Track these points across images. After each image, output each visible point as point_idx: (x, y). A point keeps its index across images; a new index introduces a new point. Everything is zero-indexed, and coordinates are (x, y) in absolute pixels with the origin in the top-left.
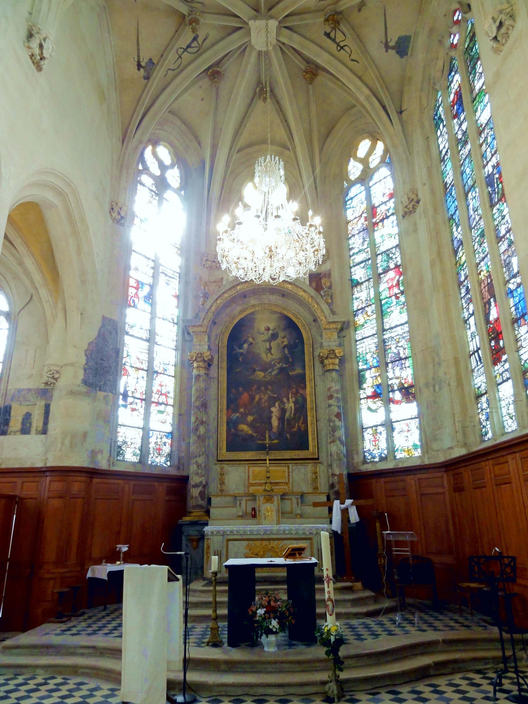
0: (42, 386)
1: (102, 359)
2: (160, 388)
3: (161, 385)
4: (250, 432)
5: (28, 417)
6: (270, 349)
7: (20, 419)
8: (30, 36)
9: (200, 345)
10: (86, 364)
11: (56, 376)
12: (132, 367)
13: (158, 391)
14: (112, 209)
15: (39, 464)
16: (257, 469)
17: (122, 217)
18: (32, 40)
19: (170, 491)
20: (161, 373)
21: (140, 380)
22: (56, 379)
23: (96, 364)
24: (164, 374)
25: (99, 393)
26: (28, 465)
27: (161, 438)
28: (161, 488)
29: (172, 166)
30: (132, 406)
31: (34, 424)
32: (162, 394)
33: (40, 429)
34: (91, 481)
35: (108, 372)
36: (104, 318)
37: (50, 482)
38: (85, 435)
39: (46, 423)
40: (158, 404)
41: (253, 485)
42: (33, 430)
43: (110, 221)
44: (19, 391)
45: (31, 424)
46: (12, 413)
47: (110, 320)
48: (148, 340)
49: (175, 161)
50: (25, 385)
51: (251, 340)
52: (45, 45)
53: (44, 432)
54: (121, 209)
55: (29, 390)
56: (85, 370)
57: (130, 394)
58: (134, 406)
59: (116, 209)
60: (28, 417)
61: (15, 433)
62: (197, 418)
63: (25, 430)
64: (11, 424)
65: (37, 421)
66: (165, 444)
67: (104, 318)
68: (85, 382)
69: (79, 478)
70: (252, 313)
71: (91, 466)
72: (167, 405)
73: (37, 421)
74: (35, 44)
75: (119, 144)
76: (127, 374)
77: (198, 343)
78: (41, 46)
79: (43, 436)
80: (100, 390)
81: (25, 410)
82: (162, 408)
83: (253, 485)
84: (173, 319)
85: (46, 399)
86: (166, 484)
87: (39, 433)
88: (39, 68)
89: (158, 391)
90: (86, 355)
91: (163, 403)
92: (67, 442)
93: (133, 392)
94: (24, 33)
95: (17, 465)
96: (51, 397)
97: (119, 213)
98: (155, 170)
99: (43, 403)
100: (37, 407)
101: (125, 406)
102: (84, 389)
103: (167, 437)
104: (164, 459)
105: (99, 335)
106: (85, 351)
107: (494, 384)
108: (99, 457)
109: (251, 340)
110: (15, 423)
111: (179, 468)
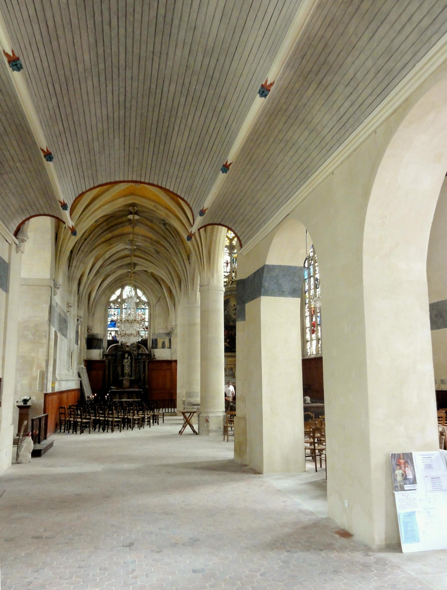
4: (228, 345)
5: (163, 343)
6: (235, 313)
7: (161, 343)
15: (169, 359)
16: (230, 359)
26: (166, 359)
33: (169, 346)
41: (229, 365)
44: (160, 333)
51: (228, 309)
55: (163, 333)
60: (163, 343)
61: (160, 348)
63: (163, 347)
65: (167, 344)
70: (228, 299)
73: (167, 344)
79: (170, 349)
83: (229, 365)
87: (168, 348)
95: (162, 359)
99: (168, 338)
107: (312, 340)
109: (228, 309)
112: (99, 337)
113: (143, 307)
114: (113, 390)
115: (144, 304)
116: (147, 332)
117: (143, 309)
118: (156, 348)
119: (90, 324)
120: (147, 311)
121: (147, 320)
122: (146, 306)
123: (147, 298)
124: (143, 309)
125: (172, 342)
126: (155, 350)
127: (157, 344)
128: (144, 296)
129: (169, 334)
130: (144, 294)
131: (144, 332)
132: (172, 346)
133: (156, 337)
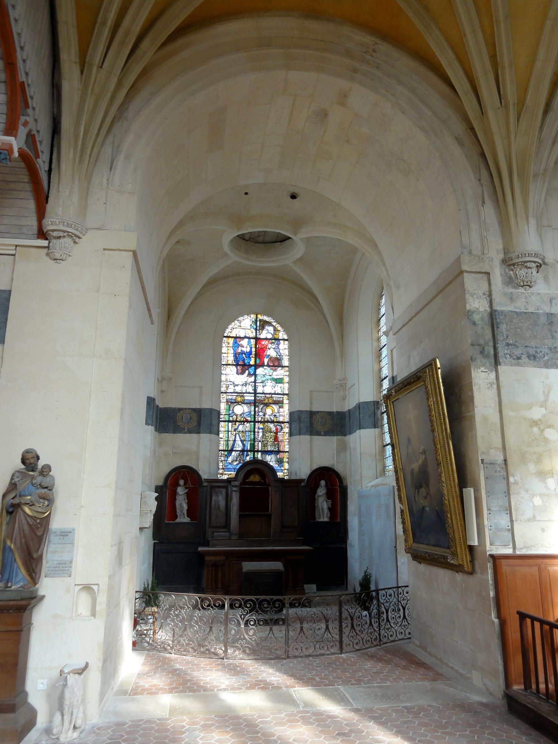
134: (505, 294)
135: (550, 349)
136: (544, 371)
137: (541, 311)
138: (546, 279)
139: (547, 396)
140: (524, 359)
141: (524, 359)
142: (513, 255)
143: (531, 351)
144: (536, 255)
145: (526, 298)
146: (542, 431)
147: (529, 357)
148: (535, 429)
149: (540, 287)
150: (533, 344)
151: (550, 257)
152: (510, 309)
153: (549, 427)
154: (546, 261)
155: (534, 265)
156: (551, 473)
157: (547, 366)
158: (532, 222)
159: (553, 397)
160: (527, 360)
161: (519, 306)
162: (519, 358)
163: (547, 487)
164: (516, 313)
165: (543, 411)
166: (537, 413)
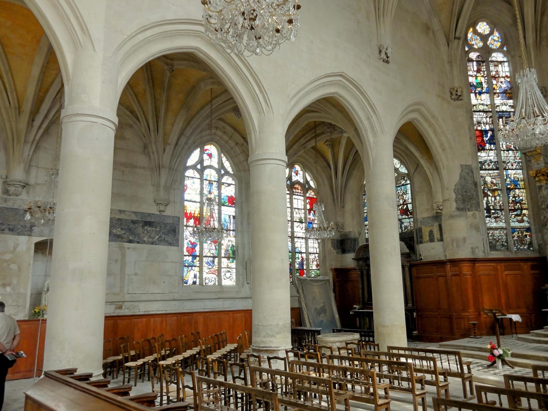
0: (435, 215)
1: (466, 192)
2: (514, 199)
3: (514, 197)
5: (431, 232)
7: (427, 234)
8: (380, 52)
9: (538, 164)
10: (456, 198)
11: (441, 208)
12: (489, 190)
13: (513, 201)
14: (452, 94)
15: (443, 258)
17: (460, 96)
18: (382, 54)
19: (533, 268)
20: (512, 189)
21: (498, 198)
22: (441, 210)
23: (462, 196)
24: (516, 189)
25: (468, 212)
26: (437, 259)
27: (522, 233)
28: (526, 267)
29: (491, 33)
30: (494, 215)
31: (436, 237)
32: (517, 203)
33: (439, 238)
34: (474, 265)
35: (472, 198)
36: (461, 166)
37: (450, 267)
38: (464, 239)
39: (441, 235)
40: (515, 210)
42: (436, 240)
43: (453, 101)
44: (423, 218)
45: (433, 236)
46: (423, 231)
47: (466, 166)
48: (497, 169)
49: (493, 26)
50: (426, 215)
52: (388, 52)
53: (441, 240)
54: (457, 91)
55: (428, 217)
56: (456, 202)
57: (491, 207)
58: (496, 215)
59: (454, 93)
60: (431, 232)
61: (427, 242)
62: (545, 217)
63: (432, 240)
64: (424, 237)
65: (437, 235)
66: (526, 236)
67: (461, 166)
68: (458, 209)
69: (466, 265)
71: (472, 257)
72: (522, 209)
73: (437, 235)
74: (383, 56)
75: (446, 48)
76: (486, 195)
77: (535, 163)
78: (386, 54)
80: (469, 211)
81: (429, 229)
82: (519, 212)
84: (515, 148)
85: (438, 222)
86: (529, 264)
88: (388, 62)
89: (513, 201)
90: (455, 193)
91: (518, 209)
92: (455, 245)
93: (493, 206)
94: (378, 51)
96: (441, 220)
97: (456, 95)
98: (478, 43)
99: (437, 224)
100: (435, 226)
101: (490, 217)
102: (458, 213)
103: (527, 232)
104: (526, 246)
105: (460, 178)
106: (454, 190)
108: (477, 251)
110: (426, 237)
111: (540, 253)
112: (352, 236)
113: (403, 182)
114: (356, 310)
115: (404, 177)
116: (412, 220)
117: (403, 185)
118: (421, 243)
119: (340, 220)
120: (409, 186)
121: (410, 201)
122: (407, 180)
123: (407, 168)
124: (403, 185)
125: (443, 232)
126: (421, 245)
127: (421, 237)
128: (402, 166)
129: (437, 217)
130: (402, 162)
131: (408, 220)
132: (444, 236)
133: (419, 226)
134: (2, 198)
135: (22, 226)
136: (17, 237)
137: (21, 208)
138: (28, 193)
139: (15, 248)
140: (7, 230)
141: (7, 230)
142: (8, 180)
143: (11, 227)
144: (20, 182)
145: (14, 201)
146: (9, 265)
147: (9, 230)
148: (5, 264)
149: (24, 196)
150: (13, 223)
151: (32, 181)
152: (3, 206)
153: (13, 263)
154: (29, 183)
155: (19, 186)
156: (9, 285)
157: (19, 234)
158: (22, 165)
159: (18, 249)
160: (8, 231)
161: (10, 205)
162: (3, 230)
163: (6, 291)
164: (7, 208)
165: (12, 255)
166: (8, 257)
